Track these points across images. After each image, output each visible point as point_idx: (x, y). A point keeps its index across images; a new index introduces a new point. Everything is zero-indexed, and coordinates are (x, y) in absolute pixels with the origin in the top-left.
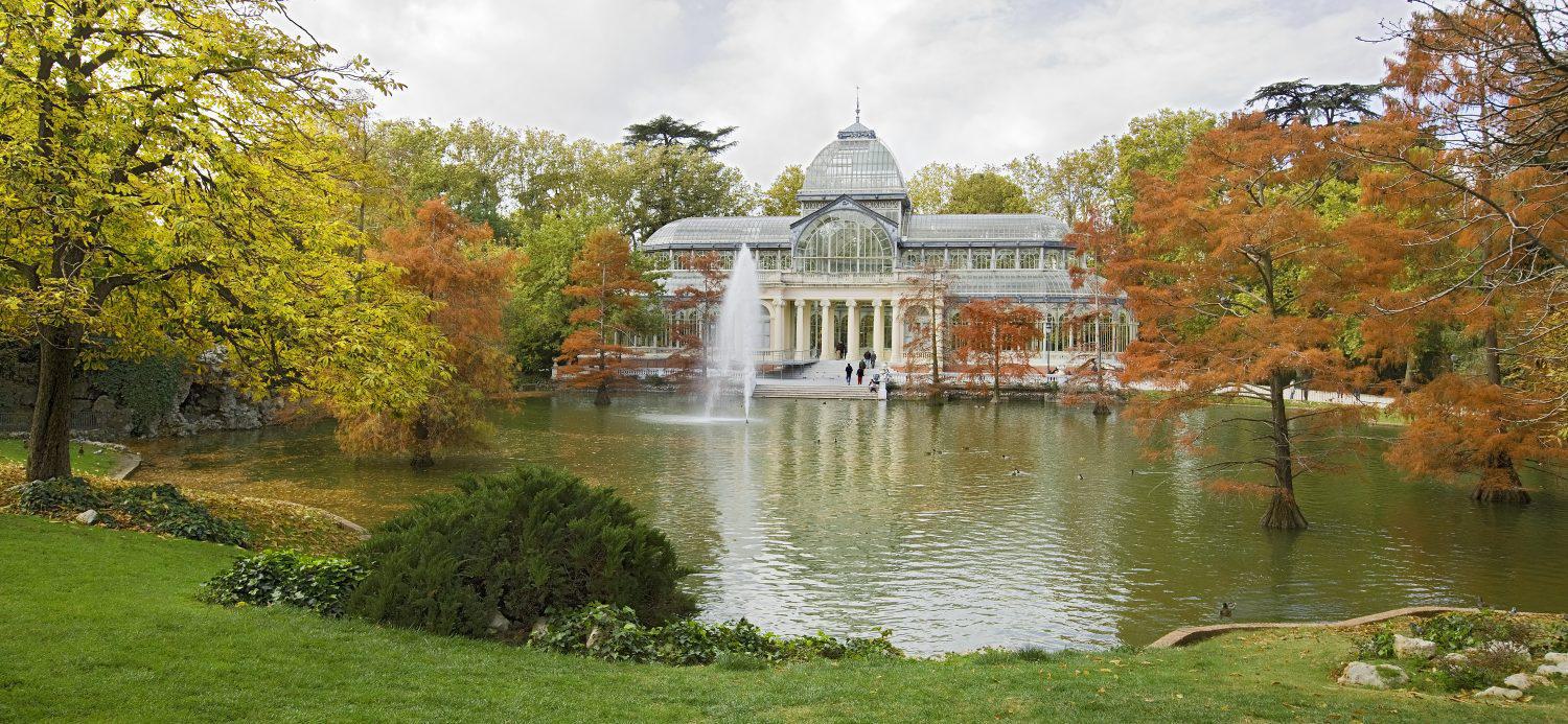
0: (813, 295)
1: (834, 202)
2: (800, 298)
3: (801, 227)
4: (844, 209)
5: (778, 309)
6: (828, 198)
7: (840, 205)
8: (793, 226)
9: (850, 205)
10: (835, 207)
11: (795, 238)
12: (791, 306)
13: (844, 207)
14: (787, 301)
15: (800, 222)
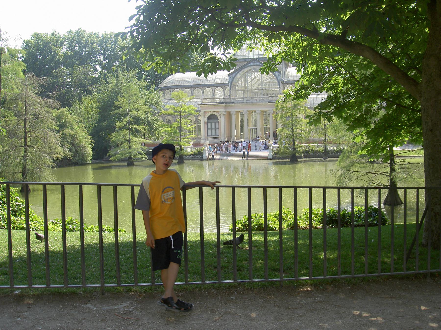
0: (240, 109)
1: (250, 62)
2: (233, 110)
3: (233, 75)
4: (254, 65)
5: (222, 117)
6: (247, 60)
7: (251, 64)
8: (229, 75)
9: (257, 63)
10: (250, 64)
11: (230, 81)
12: (229, 115)
13: (254, 64)
14: (228, 112)
15: (233, 73)
